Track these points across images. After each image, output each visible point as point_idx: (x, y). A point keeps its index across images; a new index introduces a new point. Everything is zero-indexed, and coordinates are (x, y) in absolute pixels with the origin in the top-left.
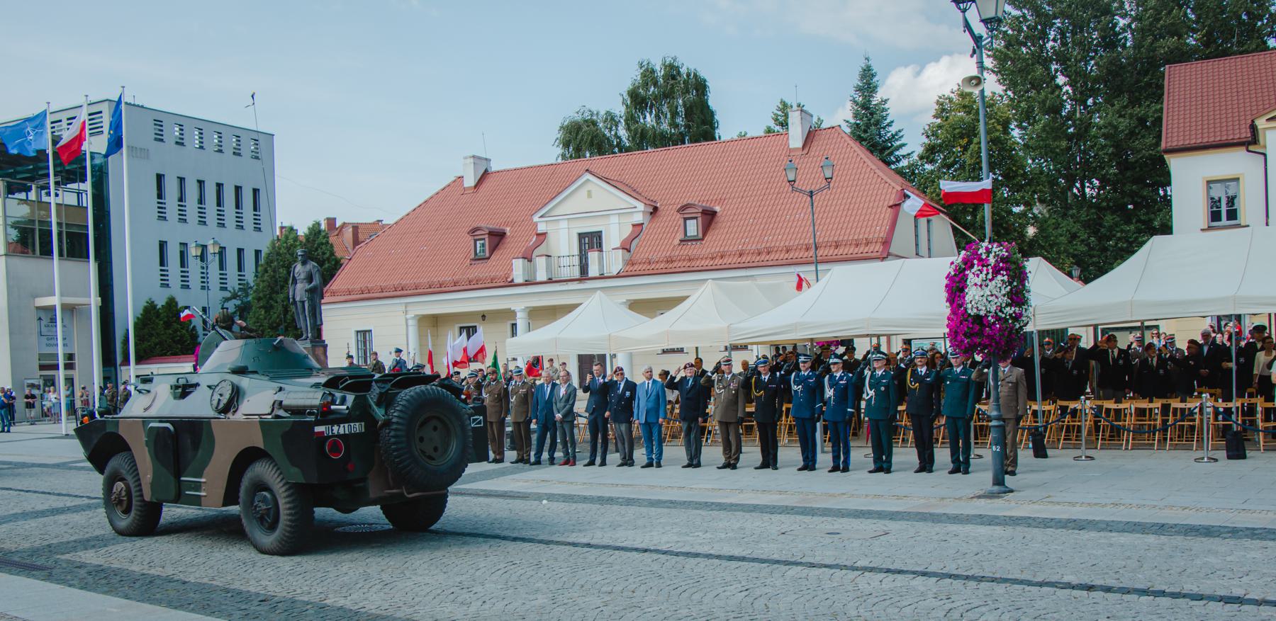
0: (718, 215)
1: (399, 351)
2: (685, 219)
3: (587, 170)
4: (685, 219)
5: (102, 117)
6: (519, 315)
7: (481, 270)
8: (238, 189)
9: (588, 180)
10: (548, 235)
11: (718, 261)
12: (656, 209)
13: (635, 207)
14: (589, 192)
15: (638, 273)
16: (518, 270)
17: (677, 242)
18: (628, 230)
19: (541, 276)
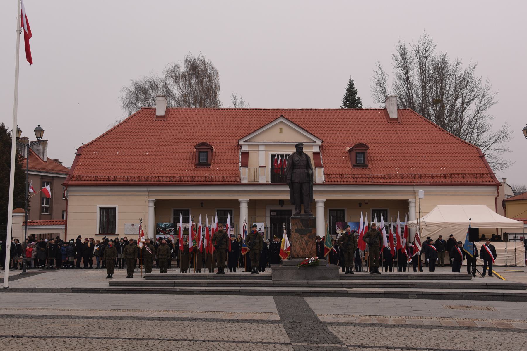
3: (282, 116)
7: (203, 173)
9: (281, 122)
11: (389, 180)
15: (336, 183)
16: (245, 175)
17: (350, 166)
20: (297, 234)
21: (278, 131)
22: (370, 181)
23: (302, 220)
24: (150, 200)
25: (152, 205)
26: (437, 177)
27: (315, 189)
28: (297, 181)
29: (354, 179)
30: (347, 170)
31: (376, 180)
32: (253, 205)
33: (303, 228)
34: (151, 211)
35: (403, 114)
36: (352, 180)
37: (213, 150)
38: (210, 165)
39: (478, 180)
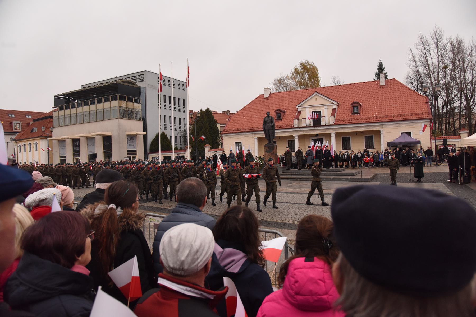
0: (362, 106)
1: (231, 151)
2: (354, 107)
3: (316, 92)
4: (354, 107)
5: (136, 77)
6: (295, 137)
8: (179, 99)
9: (316, 95)
10: (301, 112)
12: (338, 103)
13: (334, 103)
14: (316, 98)
16: (296, 123)
17: (350, 114)
18: (331, 111)
19: (304, 125)
20: (266, 153)
21: (315, 99)
22: (358, 121)
23: (268, 147)
24: (255, 138)
25: (256, 140)
26: (396, 116)
27: (276, 131)
28: (267, 129)
29: (350, 121)
30: (348, 116)
31: (361, 121)
32: (302, 138)
33: (269, 150)
34: (256, 143)
35: (390, 82)
36: (349, 121)
37: (285, 112)
38: (282, 119)
39: (420, 116)
